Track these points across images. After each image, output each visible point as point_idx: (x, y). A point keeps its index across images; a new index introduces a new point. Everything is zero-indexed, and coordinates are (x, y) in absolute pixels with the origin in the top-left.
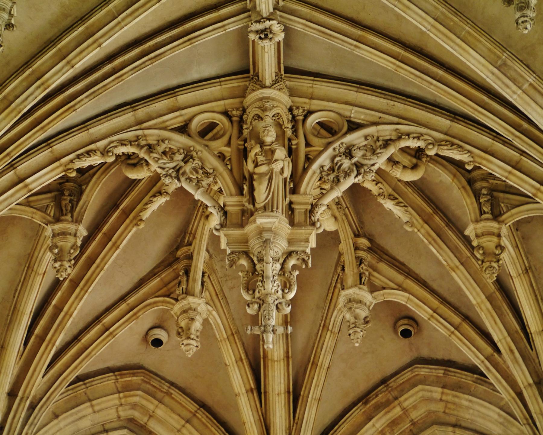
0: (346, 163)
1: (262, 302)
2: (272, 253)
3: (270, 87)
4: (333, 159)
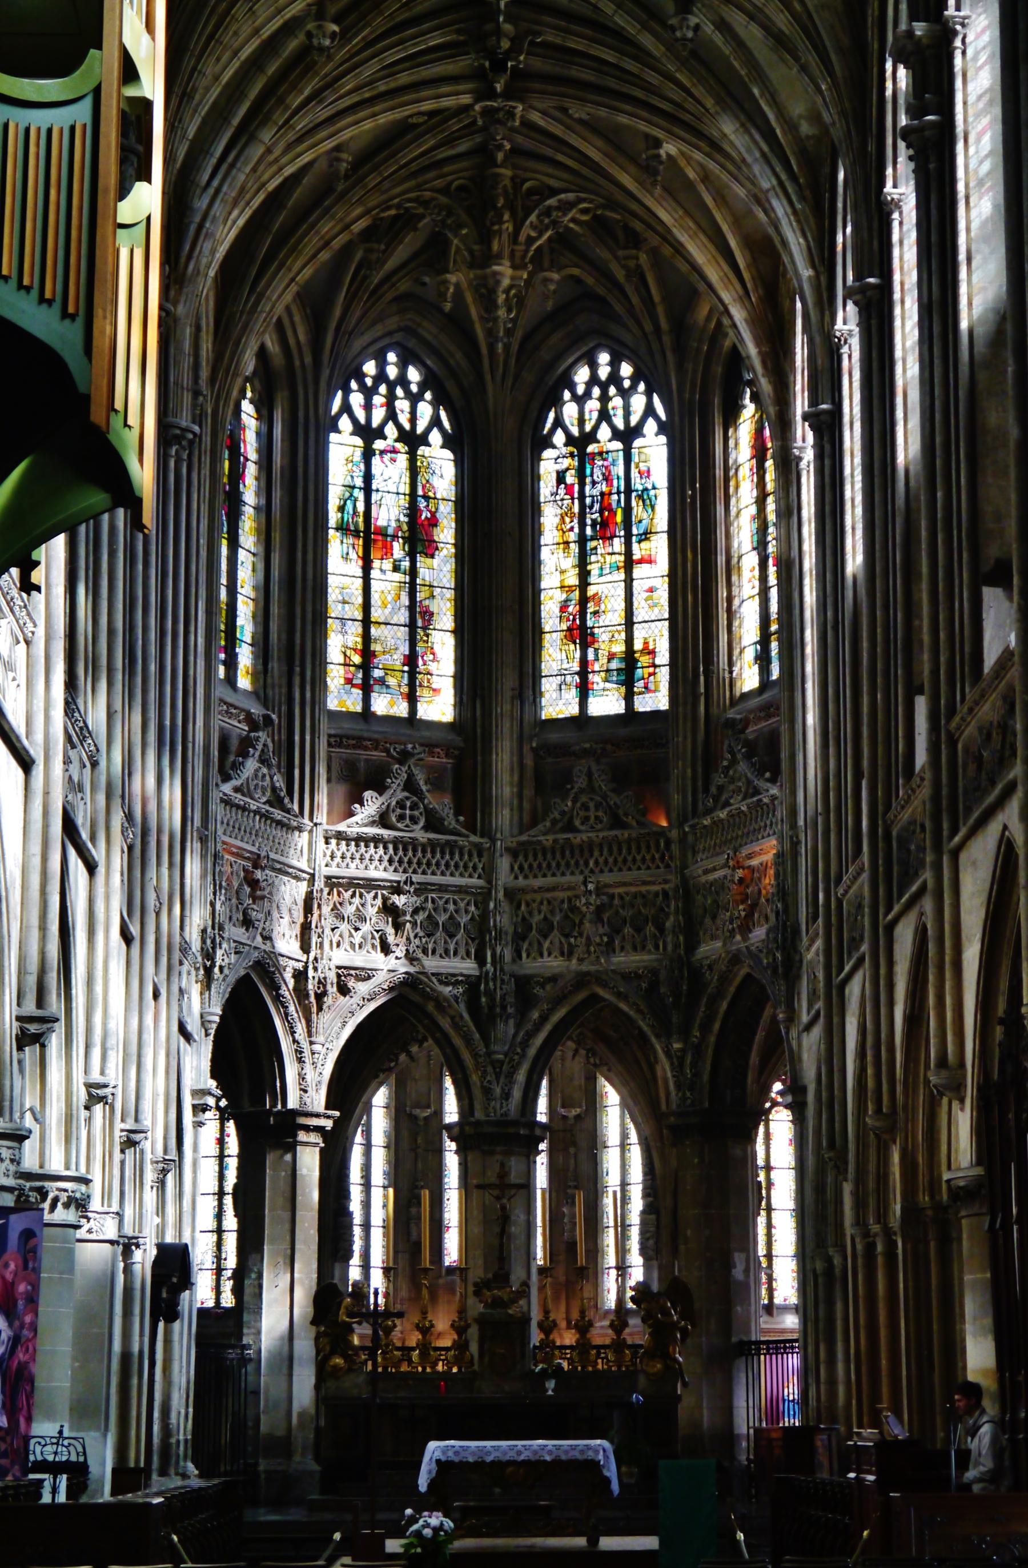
0: (546, 221)
1: (496, 319)
2: (501, 289)
3: (501, 166)
4: (538, 217)
